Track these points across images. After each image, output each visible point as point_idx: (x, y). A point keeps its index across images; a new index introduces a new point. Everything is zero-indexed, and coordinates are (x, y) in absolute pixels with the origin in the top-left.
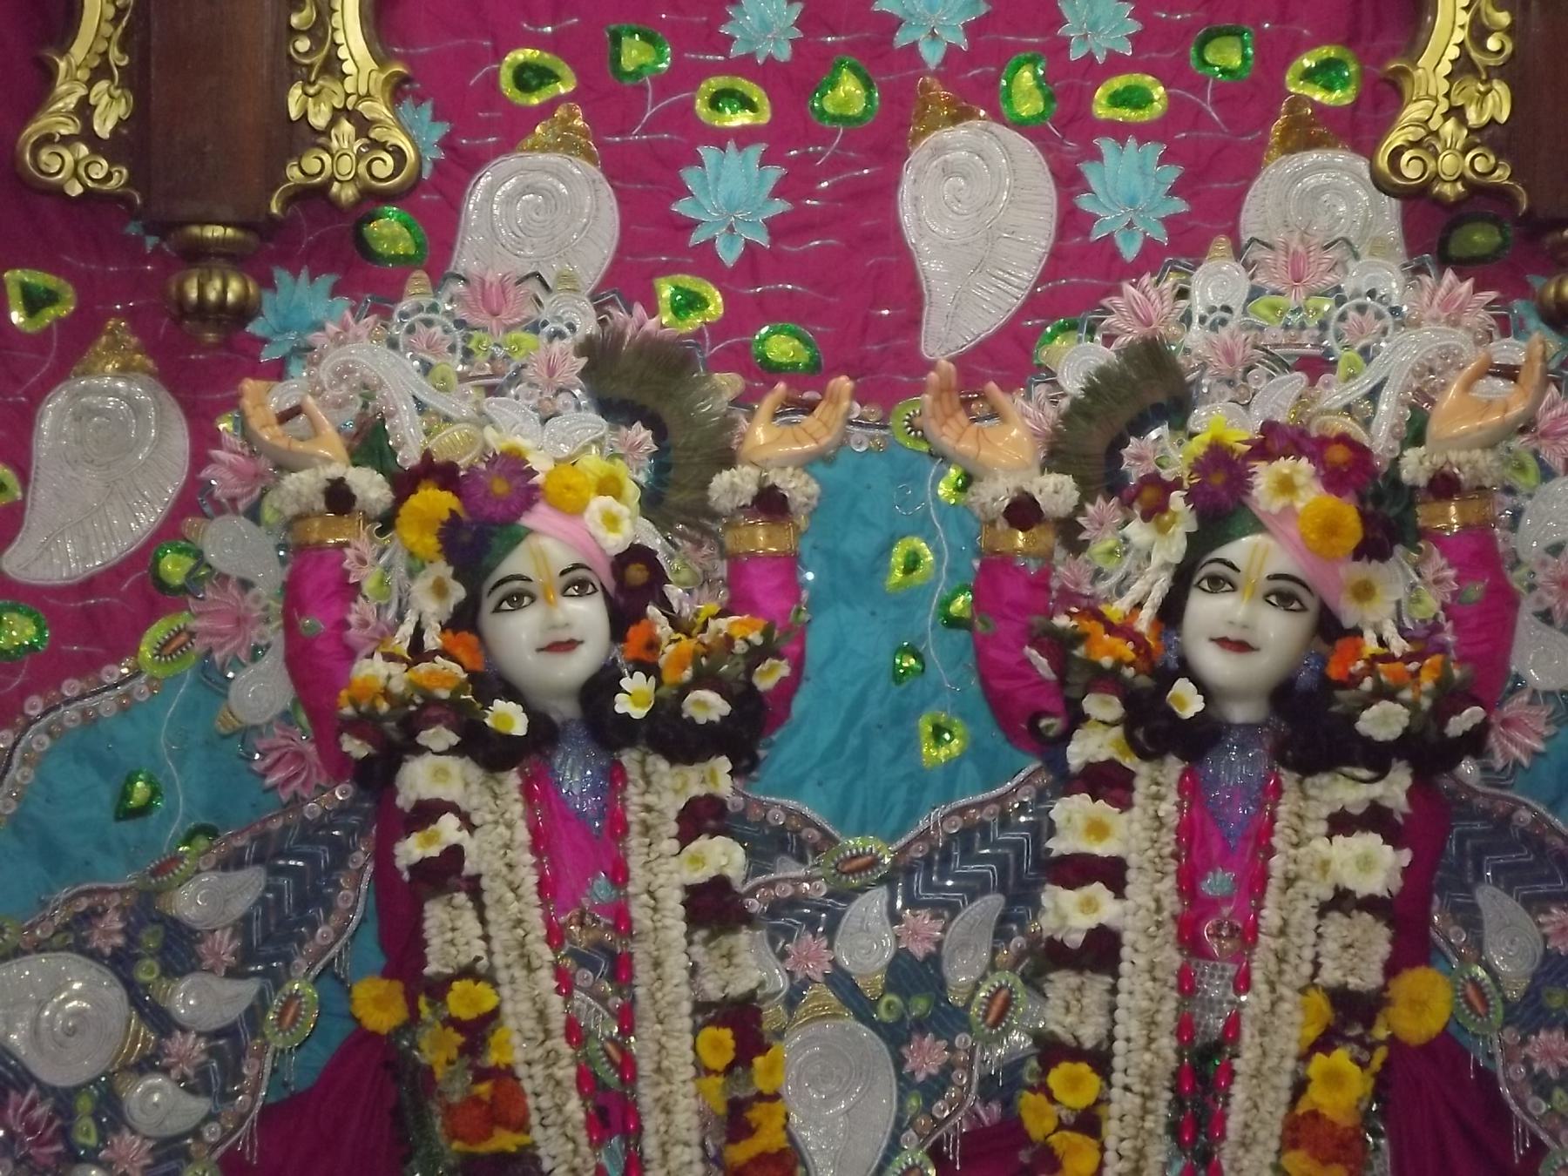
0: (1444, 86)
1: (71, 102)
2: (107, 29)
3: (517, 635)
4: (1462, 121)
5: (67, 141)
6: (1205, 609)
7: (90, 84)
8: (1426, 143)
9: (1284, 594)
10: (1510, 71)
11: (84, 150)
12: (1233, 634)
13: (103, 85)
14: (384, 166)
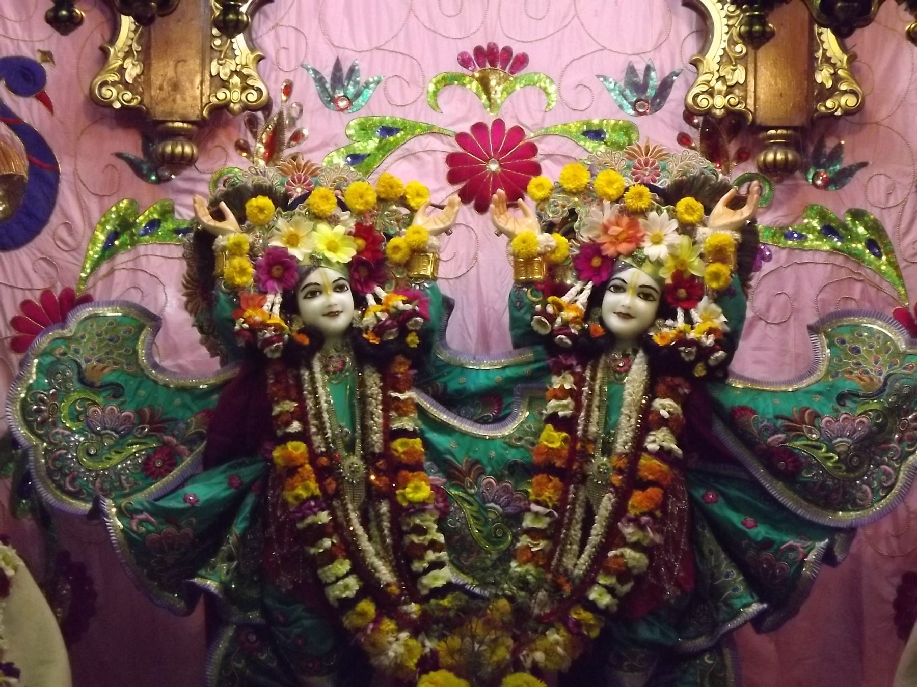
0: (717, 67)
2: (132, 35)
3: (313, 306)
5: (114, 84)
6: (610, 298)
7: (124, 59)
9: (644, 293)
12: (623, 311)
14: (253, 97)
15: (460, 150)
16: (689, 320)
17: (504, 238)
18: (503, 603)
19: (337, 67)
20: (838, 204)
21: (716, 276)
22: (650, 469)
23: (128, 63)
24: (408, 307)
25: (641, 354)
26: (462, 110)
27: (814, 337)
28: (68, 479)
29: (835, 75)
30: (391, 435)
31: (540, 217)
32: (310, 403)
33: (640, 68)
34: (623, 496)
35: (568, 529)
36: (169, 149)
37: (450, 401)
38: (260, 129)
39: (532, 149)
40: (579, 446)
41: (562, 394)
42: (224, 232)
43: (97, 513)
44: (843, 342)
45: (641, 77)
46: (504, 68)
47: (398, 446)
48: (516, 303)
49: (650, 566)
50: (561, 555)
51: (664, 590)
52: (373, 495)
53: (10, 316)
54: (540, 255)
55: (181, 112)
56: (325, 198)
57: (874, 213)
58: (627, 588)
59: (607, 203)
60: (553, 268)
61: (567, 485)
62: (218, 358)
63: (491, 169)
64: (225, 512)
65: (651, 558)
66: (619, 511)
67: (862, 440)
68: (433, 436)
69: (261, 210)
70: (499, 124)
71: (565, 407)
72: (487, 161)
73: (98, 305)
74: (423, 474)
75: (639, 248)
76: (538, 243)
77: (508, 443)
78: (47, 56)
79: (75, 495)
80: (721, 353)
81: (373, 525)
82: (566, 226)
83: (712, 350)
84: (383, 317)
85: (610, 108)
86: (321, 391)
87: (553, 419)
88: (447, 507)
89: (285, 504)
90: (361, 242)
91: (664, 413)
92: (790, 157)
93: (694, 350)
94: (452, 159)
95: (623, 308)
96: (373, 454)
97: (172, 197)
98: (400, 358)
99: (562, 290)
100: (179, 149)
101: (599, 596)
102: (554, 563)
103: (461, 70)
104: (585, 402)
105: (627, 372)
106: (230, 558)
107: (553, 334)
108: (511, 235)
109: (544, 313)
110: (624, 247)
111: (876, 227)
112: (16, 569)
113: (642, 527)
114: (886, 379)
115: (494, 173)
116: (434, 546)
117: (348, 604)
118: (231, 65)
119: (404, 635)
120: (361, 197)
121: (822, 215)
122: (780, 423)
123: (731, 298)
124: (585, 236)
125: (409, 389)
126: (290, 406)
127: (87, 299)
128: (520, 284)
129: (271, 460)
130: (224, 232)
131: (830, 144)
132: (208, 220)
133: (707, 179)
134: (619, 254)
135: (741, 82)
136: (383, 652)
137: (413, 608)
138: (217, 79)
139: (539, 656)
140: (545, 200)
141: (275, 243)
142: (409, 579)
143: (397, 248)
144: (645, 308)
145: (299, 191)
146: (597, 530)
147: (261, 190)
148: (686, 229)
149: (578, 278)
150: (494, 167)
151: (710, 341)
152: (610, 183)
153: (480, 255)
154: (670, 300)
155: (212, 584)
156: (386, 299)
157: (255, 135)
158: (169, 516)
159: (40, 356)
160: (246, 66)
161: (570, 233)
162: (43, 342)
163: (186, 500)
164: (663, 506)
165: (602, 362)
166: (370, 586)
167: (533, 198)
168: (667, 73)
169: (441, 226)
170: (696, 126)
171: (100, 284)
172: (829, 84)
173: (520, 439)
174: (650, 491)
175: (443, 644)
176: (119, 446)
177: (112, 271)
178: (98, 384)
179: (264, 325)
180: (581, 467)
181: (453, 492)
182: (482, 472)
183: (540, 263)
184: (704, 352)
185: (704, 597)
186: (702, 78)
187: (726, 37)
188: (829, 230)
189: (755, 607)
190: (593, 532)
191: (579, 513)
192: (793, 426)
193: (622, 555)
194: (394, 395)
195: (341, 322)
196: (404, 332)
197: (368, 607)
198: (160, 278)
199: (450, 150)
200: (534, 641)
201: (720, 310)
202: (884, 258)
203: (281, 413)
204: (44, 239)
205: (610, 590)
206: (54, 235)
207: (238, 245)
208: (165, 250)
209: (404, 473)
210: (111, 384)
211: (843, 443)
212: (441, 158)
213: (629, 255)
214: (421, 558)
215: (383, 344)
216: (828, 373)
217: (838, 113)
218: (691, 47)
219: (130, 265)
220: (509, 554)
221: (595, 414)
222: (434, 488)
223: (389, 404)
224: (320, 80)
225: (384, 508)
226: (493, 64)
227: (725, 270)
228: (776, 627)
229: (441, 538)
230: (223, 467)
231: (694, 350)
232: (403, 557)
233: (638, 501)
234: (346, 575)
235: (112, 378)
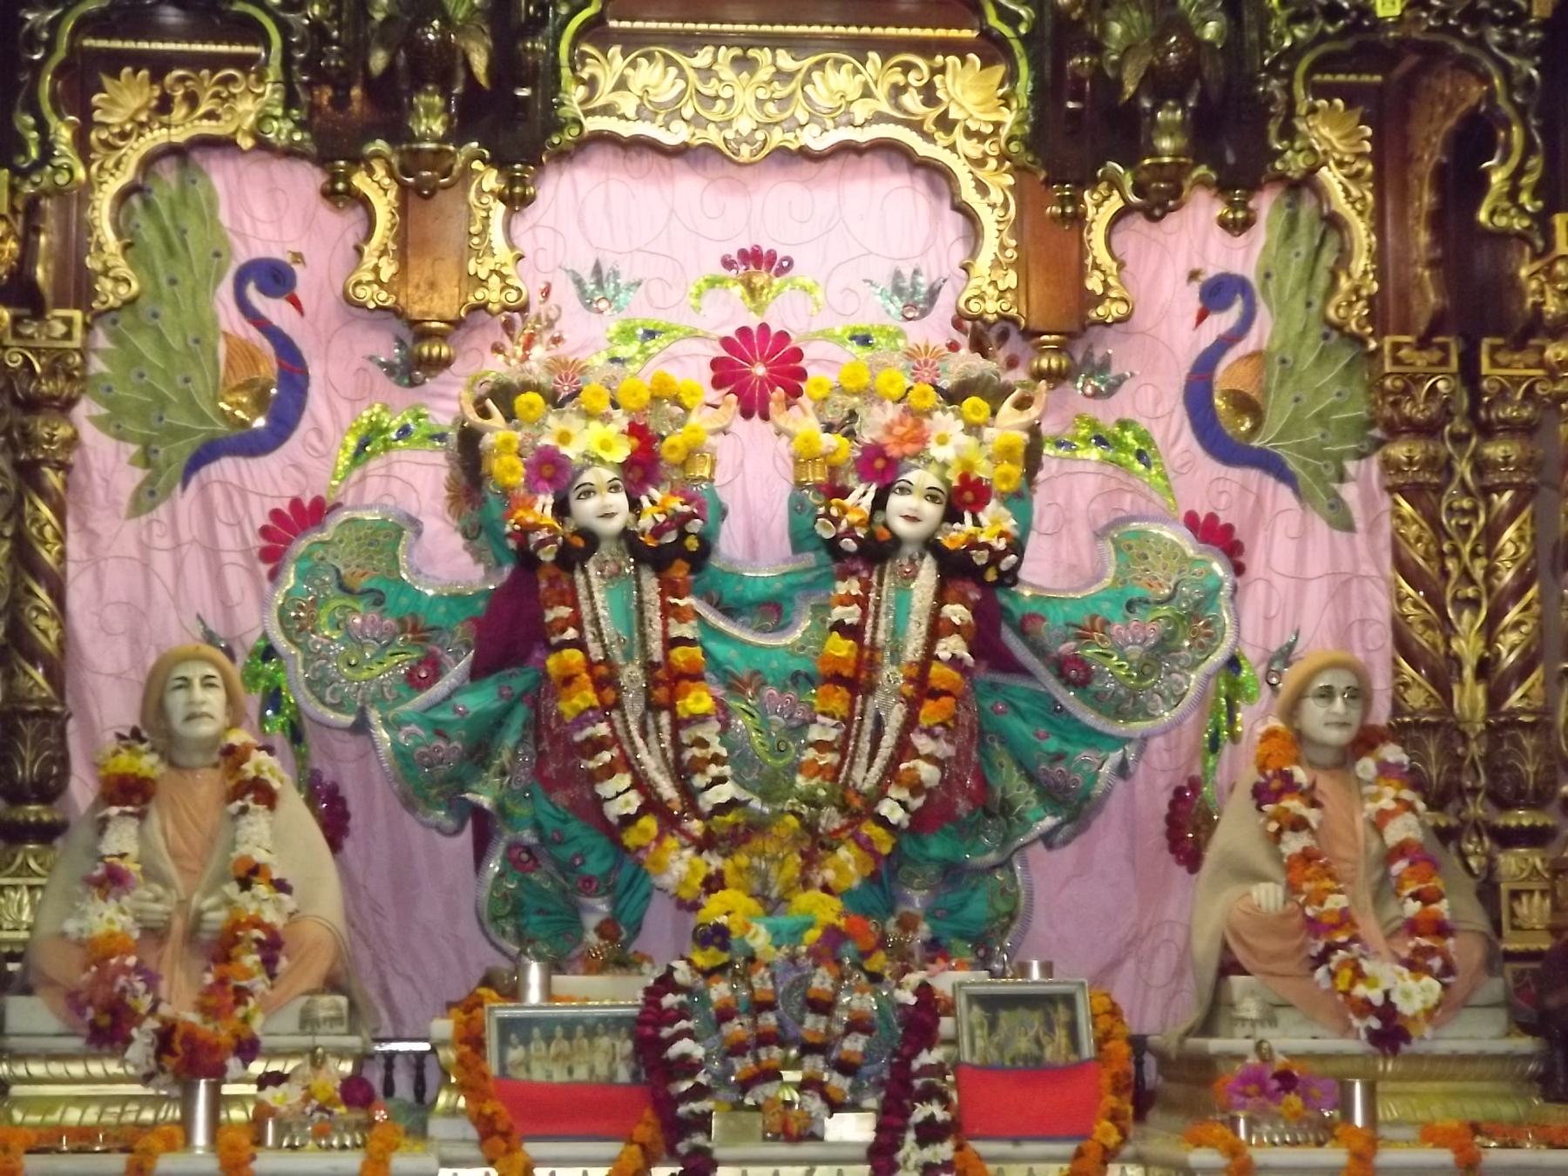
3: (586, 510)
4: (996, 287)
5: (369, 283)
6: (896, 502)
8: (981, 297)
10: (1015, 265)
11: (376, 287)
13: (384, 259)
14: (513, 296)
15: (724, 354)
16: (976, 523)
17: (785, 439)
18: (792, 821)
19: (597, 270)
20: (1106, 414)
21: (1006, 478)
22: (942, 678)
23: (383, 262)
24: (687, 509)
25: (929, 558)
26: (729, 312)
27: (1100, 544)
28: (328, 690)
29: (1105, 282)
30: (671, 643)
31: (819, 417)
32: (585, 608)
33: (907, 272)
34: (913, 705)
35: (857, 741)
36: (425, 350)
37: (729, 612)
38: (517, 333)
39: (798, 354)
40: (867, 654)
41: (847, 600)
42: (492, 430)
43: (361, 727)
44: (1130, 548)
45: (907, 284)
46: (769, 270)
47: (679, 655)
48: (797, 507)
49: (942, 781)
50: (850, 768)
51: (956, 804)
52: (653, 707)
53: (258, 525)
54: (824, 456)
55: (438, 311)
56: (597, 395)
57: (1144, 424)
58: (917, 803)
59: (889, 403)
60: (833, 470)
61: (854, 695)
62: (481, 567)
63: (759, 371)
64: (498, 721)
65: (943, 770)
66: (910, 723)
67: (1153, 648)
68: (712, 646)
69: (531, 406)
70: (764, 328)
71: (851, 614)
72: (752, 364)
73: (354, 508)
74: (703, 684)
75: (925, 450)
76: (820, 443)
77: (792, 651)
78: (298, 257)
79: (336, 707)
80: (1012, 558)
81: (652, 738)
82: (846, 426)
83: (1004, 554)
84: (661, 518)
85: (880, 311)
86: (596, 595)
87: (839, 626)
88: (729, 718)
89: (560, 716)
90: (635, 442)
91: (956, 621)
92: (1064, 363)
93: (986, 553)
94: (715, 364)
95: (912, 512)
96: (652, 663)
97: (426, 401)
98: (679, 563)
99: (844, 493)
100: (435, 351)
101: (890, 809)
102: (842, 776)
103: (723, 272)
104: (872, 608)
105: (914, 577)
106: (503, 773)
107: (836, 539)
108: (791, 436)
109: (827, 515)
110: (909, 448)
111: (1144, 438)
112: (282, 781)
113: (934, 737)
114: (1176, 585)
115: (762, 379)
116: (716, 760)
117: (628, 820)
118: (490, 263)
119: (688, 853)
120: (634, 394)
121: (1093, 424)
122: (1072, 630)
123: (1019, 499)
124: (867, 437)
125: (688, 594)
126: (565, 611)
127: (338, 506)
128: (799, 485)
129: (545, 668)
130: (492, 430)
131: (1098, 354)
132: (473, 417)
133: (990, 379)
134: (904, 455)
135: (1014, 286)
136: (663, 868)
137: (696, 826)
138: (476, 282)
139: (829, 875)
140: (825, 399)
141: (547, 440)
142: (689, 795)
143: (673, 448)
144: (932, 511)
145: (565, 391)
146: (888, 741)
147: (526, 387)
148: (973, 429)
149: (861, 480)
150: (760, 370)
151: (1001, 545)
152: (892, 383)
153: (746, 463)
154: (956, 502)
155: (486, 801)
156: (660, 502)
157: (511, 337)
158: (439, 731)
159: (296, 561)
160: (505, 264)
161: (850, 434)
162: (301, 546)
163: (456, 711)
164: (955, 718)
165: (888, 566)
166: (653, 804)
167: (811, 398)
168: (934, 278)
169: (719, 425)
170: (965, 333)
171: (351, 493)
172: (1099, 291)
173: (803, 648)
174: (944, 700)
175: (729, 861)
176: (378, 657)
177: (363, 478)
178: (358, 590)
179: (537, 527)
180: (869, 676)
181: (734, 704)
182: (764, 684)
183: (822, 464)
184: (996, 557)
185: (995, 810)
186: (974, 282)
187: (997, 242)
188: (1100, 441)
189: (1049, 822)
190: (883, 744)
191: (869, 724)
192: (1084, 634)
193: (915, 769)
194: (673, 600)
195: (615, 525)
196: (683, 535)
197: (649, 823)
198: (419, 481)
199: (715, 354)
200: (823, 859)
201: (1009, 513)
202: (1154, 471)
203: (556, 619)
204: (293, 445)
205: (903, 804)
206: (304, 442)
207: (507, 443)
208: (419, 456)
209: (685, 683)
210: (371, 590)
211: (1135, 652)
212: (706, 363)
213: (916, 456)
214: (703, 772)
215: (661, 547)
216: (1115, 579)
217: (1109, 320)
218: (959, 253)
219: (382, 471)
220: (797, 768)
221: (883, 622)
222: (715, 699)
223: (667, 611)
224: (579, 282)
225: (665, 719)
226: (758, 266)
227: (1016, 471)
228: (1066, 842)
229: (724, 752)
230: (491, 680)
231: (986, 553)
232: (682, 773)
233: (930, 713)
234: (627, 790)
235: (373, 585)
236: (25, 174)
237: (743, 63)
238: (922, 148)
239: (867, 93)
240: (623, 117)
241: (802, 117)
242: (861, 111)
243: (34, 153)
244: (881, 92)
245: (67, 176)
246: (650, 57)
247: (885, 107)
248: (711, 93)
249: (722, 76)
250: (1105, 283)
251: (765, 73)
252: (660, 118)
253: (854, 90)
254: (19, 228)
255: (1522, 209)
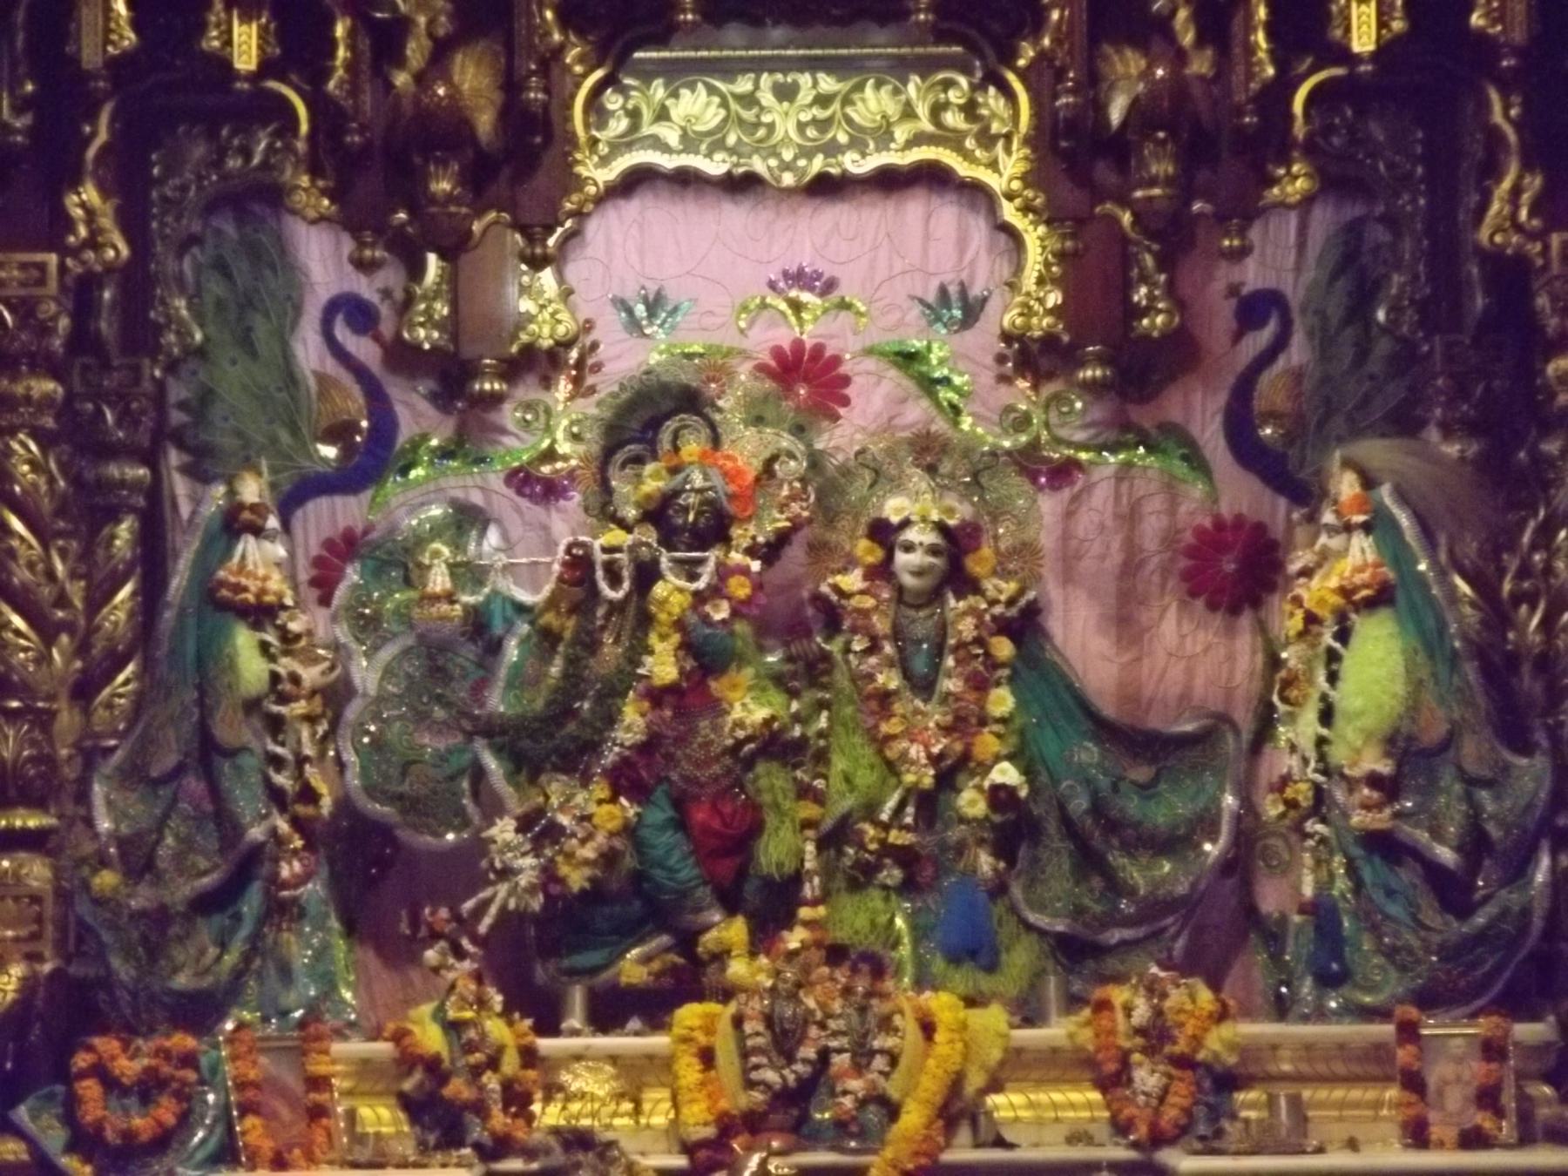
1: (422, 306)
29: (1150, 292)
100: (487, 386)
187: (1040, 259)
236: (75, 252)
237: (786, 93)
238: (963, 169)
239: (909, 113)
240: (666, 148)
241: (843, 138)
242: (901, 133)
243: (83, 231)
244: (922, 110)
245: (111, 253)
246: (692, 87)
247: (926, 125)
248: (754, 120)
249: (764, 102)
250: (1151, 297)
251: (805, 96)
252: (703, 147)
253: (892, 108)
254: (70, 306)
255: (1518, 227)
